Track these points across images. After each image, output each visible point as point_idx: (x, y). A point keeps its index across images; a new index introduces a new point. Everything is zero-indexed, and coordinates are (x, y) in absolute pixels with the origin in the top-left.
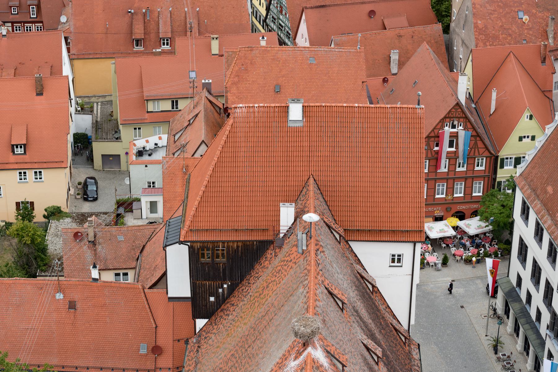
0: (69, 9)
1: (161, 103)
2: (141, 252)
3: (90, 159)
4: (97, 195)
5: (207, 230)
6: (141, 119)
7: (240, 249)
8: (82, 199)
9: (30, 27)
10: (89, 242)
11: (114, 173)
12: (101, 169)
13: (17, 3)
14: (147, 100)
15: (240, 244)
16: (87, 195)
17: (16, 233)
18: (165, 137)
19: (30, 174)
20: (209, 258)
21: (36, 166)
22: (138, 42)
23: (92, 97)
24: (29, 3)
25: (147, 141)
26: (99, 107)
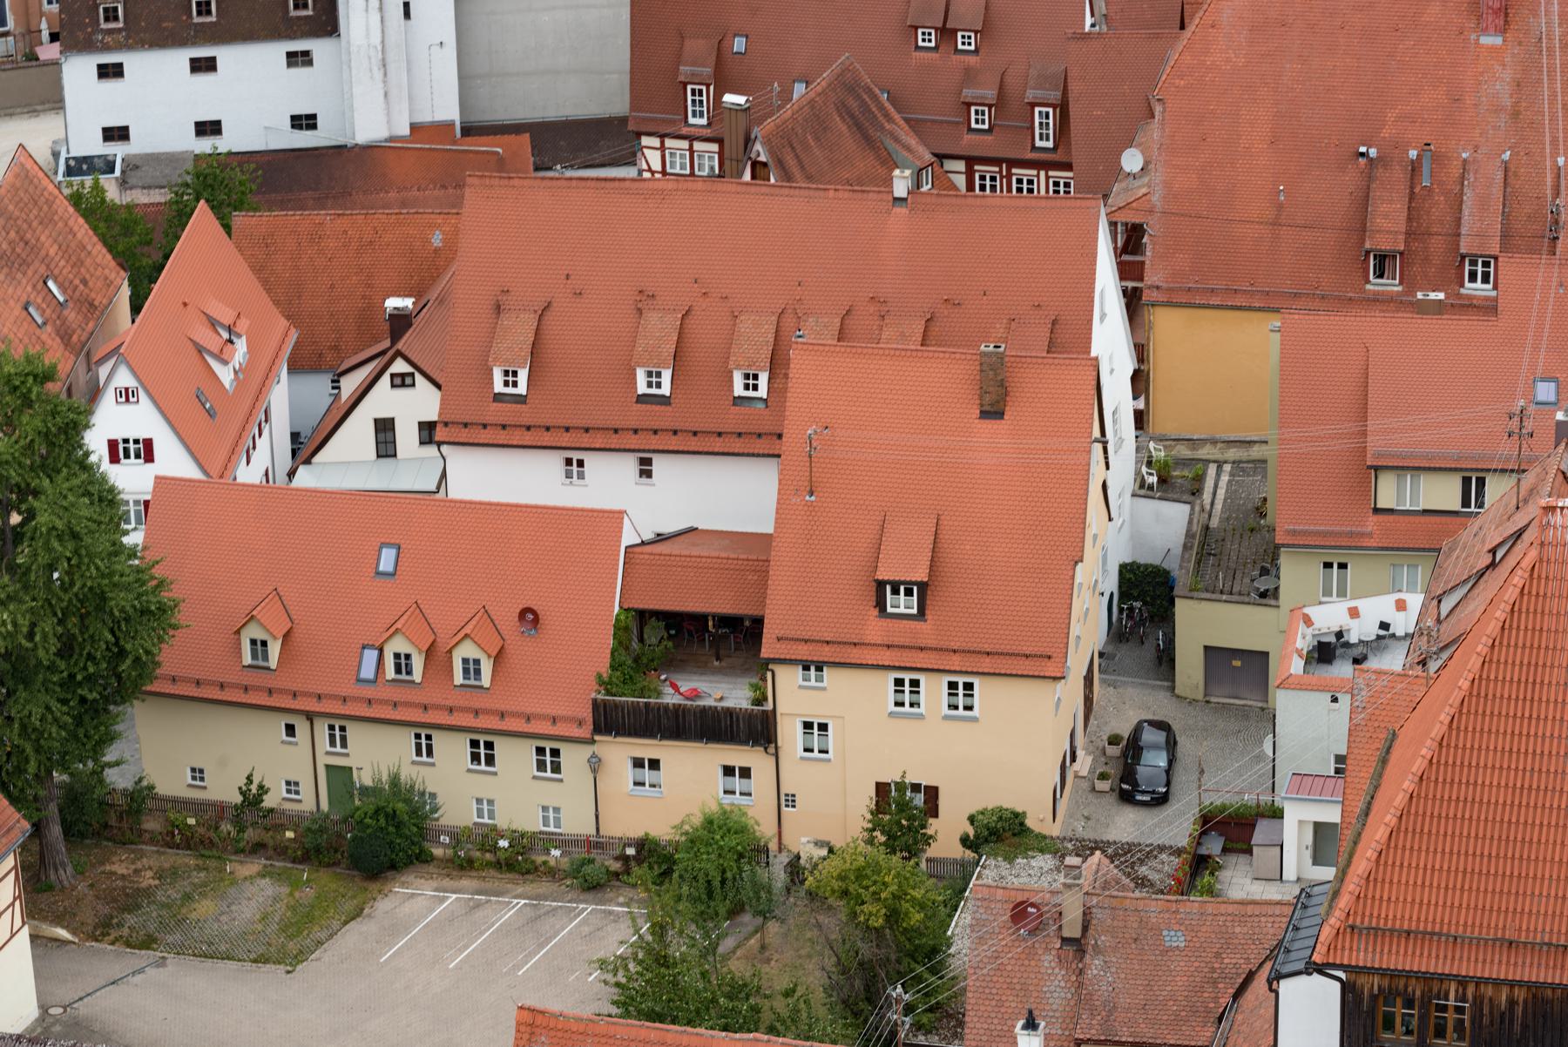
0: (1154, 132)
1: (1425, 480)
2: (1237, 995)
3: (1165, 660)
4: (1168, 784)
5: (1408, 933)
6: (1351, 535)
7: (1519, 1010)
8: (1115, 795)
9: (1030, 182)
10: (1065, 940)
11: (1244, 713)
12: (1200, 696)
13: (990, 94)
14: (1377, 469)
15: (1521, 995)
16: (1135, 784)
17: (836, 884)
18: (1415, 601)
19: (934, 690)
20: (1409, 1032)
21: (955, 662)
22: (1383, 263)
23: (1204, 441)
24: (1030, 95)
25: (1354, 613)
26: (1225, 478)
